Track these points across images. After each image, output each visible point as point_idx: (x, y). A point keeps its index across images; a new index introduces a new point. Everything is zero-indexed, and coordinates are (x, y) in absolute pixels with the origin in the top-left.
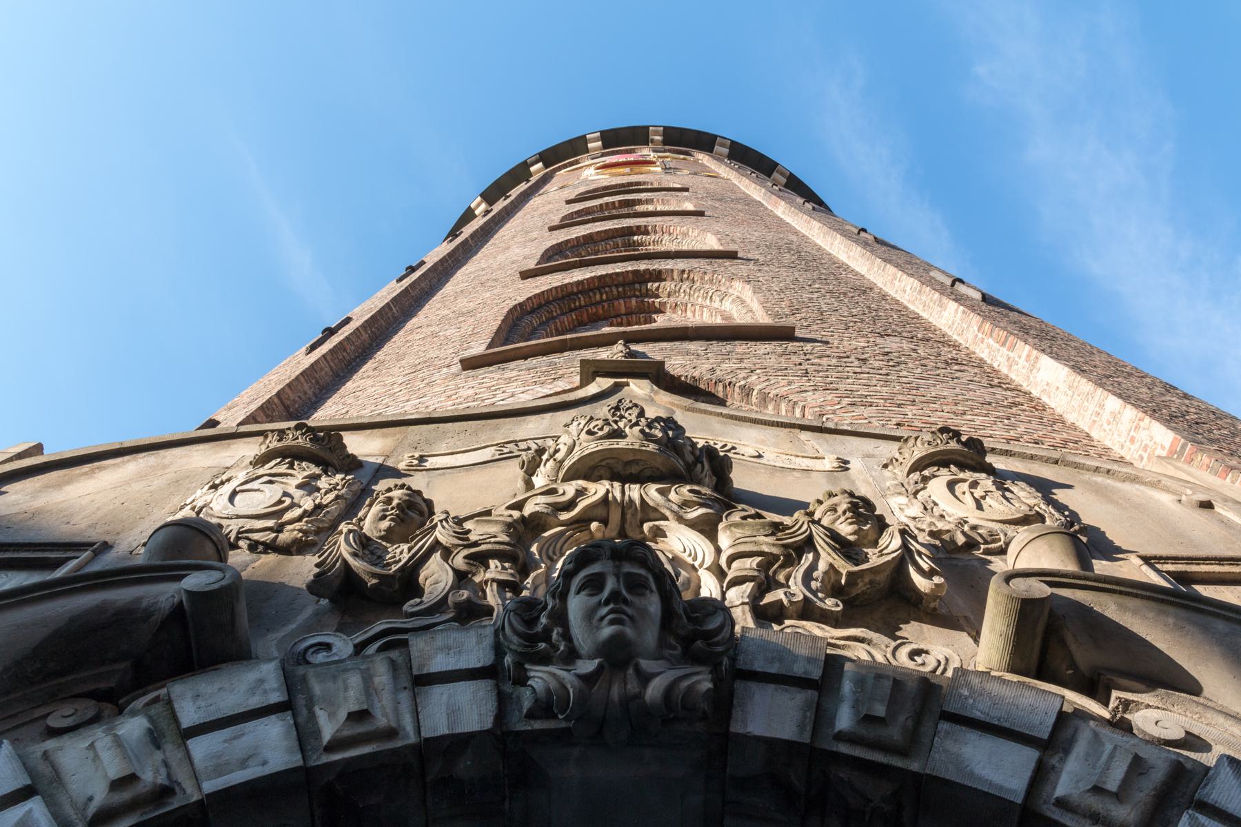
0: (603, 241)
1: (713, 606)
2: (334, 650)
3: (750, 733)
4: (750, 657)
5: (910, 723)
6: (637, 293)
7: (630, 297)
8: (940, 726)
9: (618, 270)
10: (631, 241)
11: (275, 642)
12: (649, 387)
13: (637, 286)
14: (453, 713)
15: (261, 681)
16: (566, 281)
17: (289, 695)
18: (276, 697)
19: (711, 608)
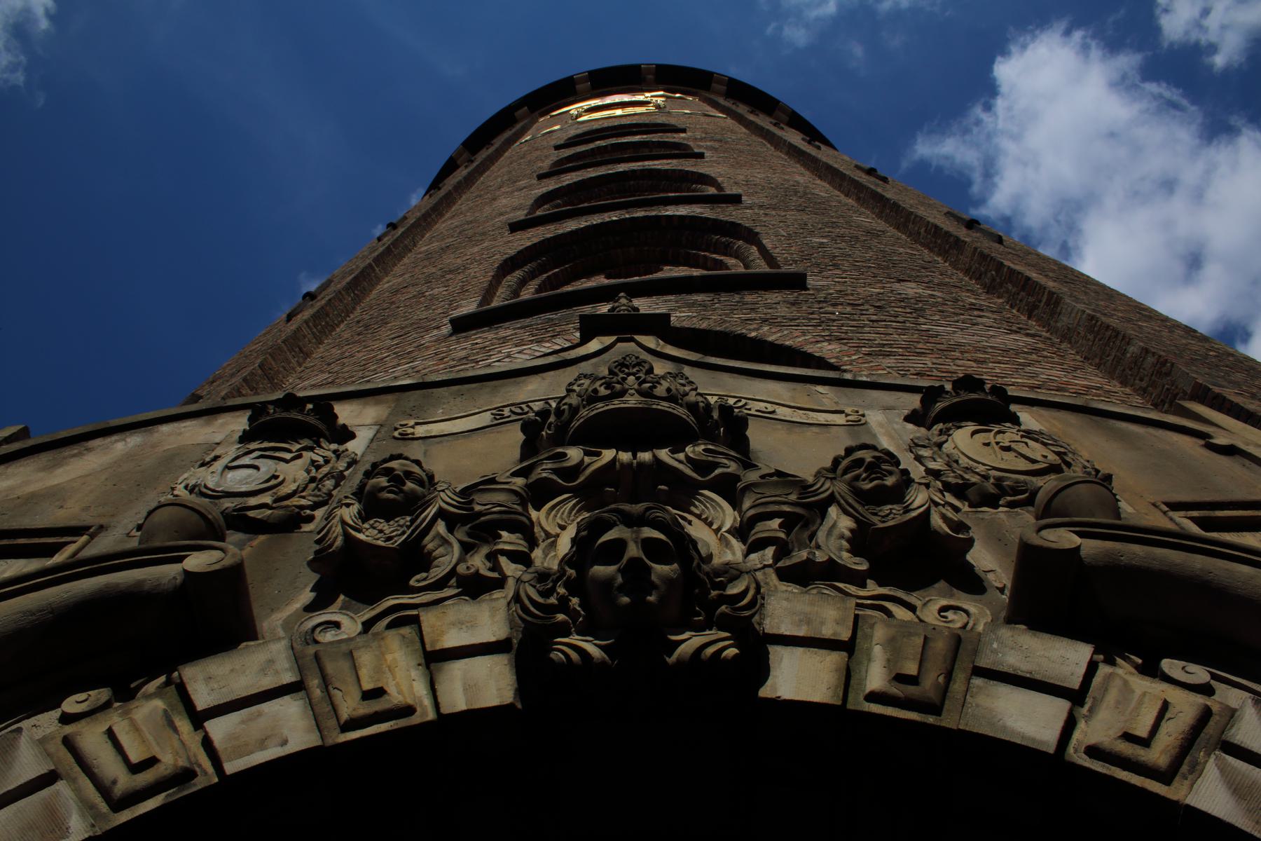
1: (737, 570)
2: (343, 629)
3: (779, 697)
4: (776, 621)
5: (941, 679)
8: (971, 681)
9: (614, 218)
11: (280, 622)
12: (655, 342)
14: (469, 688)
15: (271, 662)
16: (561, 232)
17: (301, 675)
18: (288, 678)
19: (735, 572)
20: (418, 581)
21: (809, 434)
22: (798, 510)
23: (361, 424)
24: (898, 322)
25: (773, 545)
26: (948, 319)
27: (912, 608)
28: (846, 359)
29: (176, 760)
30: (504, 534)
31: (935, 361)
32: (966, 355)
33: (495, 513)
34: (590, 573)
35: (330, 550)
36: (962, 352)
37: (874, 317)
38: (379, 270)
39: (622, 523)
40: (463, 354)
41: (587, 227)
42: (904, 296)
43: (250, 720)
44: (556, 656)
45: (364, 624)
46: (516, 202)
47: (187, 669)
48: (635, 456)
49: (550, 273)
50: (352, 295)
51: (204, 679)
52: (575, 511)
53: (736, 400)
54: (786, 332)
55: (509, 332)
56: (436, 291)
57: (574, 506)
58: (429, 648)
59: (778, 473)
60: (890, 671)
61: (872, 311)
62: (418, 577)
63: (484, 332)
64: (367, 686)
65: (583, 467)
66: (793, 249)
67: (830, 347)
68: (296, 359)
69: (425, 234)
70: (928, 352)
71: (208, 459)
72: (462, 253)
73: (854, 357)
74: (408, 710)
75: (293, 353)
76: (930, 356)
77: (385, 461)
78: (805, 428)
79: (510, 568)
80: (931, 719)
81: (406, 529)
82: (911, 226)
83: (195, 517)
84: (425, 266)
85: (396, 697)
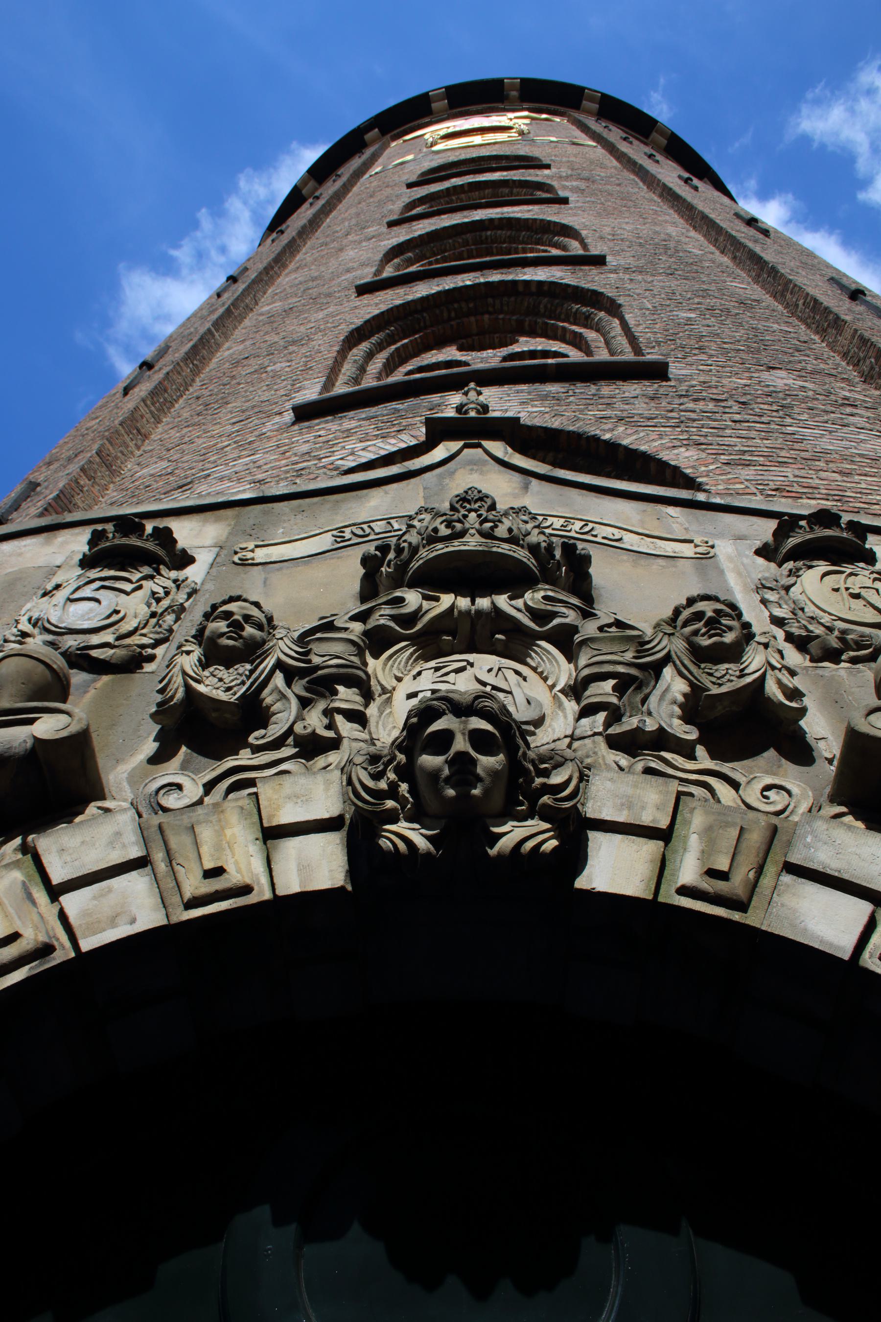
0: (450, 238)
1: (562, 757)
2: (185, 792)
3: (594, 889)
4: (599, 804)
5: (752, 875)
6: (491, 309)
7: (483, 314)
8: (781, 878)
9: (468, 283)
10: (484, 238)
11: (125, 775)
12: (503, 449)
13: (490, 300)
14: (304, 869)
15: (118, 834)
16: (410, 298)
17: (147, 849)
18: (135, 852)
19: (560, 759)
20: (257, 739)
21: (655, 567)
22: (633, 671)
23: (201, 545)
24: (763, 423)
25: (604, 711)
26: (817, 419)
27: (735, 785)
28: (703, 469)
29: (36, 935)
30: (341, 688)
31: (797, 473)
32: (831, 465)
33: (331, 666)
34: (419, 762)
35: (172, 703)
36: (827, 462)
37: (737, 417)
38: (219, 336)
39: (451, 712)
40: (305, 448)
41: (439, 293)
42: (772, 389)
43: (102, 896)
44: (385, 843)
45: (204, 785)
46: (364, 255)
47: (41, 840)
48: (473, 602)
49: (399, 344)
50: (191, 366)
51: (58, 852)
52: (411, 661)
53: (584, 523)
54: (642, 434)
55: (354, 424)
56: (278, 366)
57: (412, 654)
58: (266, 825)
59: (619, 624)
60: (703, 864)
61: (736, 408)
62: (257, 734)
63: (327, 422)
64: (209, 865)
65: (421, 613)
66: (657, 326)
67: (687, 454)
68: (134, 442)
69: (267, 290)
70: (790, 461)
71: (49, 587)
72: (306, 318)
73: (711, 467)
74: (246, 890)
75: (131, 436)
76: (793, 466)
77: (225, 603)
78: (652, 560)
79: (345, 727)
80: (736, 916)
81: (245, 679)
82: (788, 296)
83: (41, 667)
84: (267, 333)
85: (234, 877)
